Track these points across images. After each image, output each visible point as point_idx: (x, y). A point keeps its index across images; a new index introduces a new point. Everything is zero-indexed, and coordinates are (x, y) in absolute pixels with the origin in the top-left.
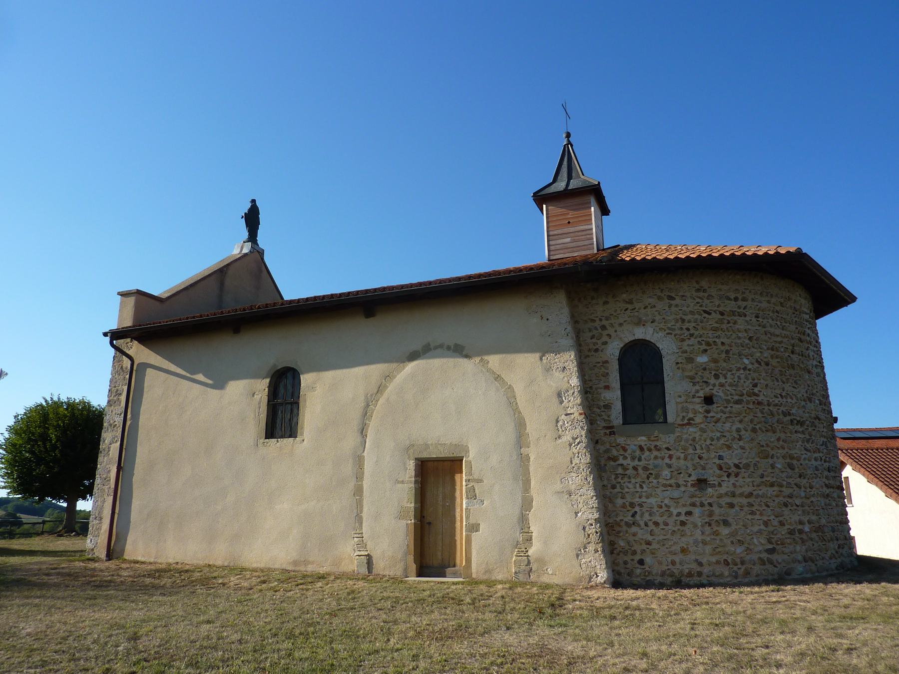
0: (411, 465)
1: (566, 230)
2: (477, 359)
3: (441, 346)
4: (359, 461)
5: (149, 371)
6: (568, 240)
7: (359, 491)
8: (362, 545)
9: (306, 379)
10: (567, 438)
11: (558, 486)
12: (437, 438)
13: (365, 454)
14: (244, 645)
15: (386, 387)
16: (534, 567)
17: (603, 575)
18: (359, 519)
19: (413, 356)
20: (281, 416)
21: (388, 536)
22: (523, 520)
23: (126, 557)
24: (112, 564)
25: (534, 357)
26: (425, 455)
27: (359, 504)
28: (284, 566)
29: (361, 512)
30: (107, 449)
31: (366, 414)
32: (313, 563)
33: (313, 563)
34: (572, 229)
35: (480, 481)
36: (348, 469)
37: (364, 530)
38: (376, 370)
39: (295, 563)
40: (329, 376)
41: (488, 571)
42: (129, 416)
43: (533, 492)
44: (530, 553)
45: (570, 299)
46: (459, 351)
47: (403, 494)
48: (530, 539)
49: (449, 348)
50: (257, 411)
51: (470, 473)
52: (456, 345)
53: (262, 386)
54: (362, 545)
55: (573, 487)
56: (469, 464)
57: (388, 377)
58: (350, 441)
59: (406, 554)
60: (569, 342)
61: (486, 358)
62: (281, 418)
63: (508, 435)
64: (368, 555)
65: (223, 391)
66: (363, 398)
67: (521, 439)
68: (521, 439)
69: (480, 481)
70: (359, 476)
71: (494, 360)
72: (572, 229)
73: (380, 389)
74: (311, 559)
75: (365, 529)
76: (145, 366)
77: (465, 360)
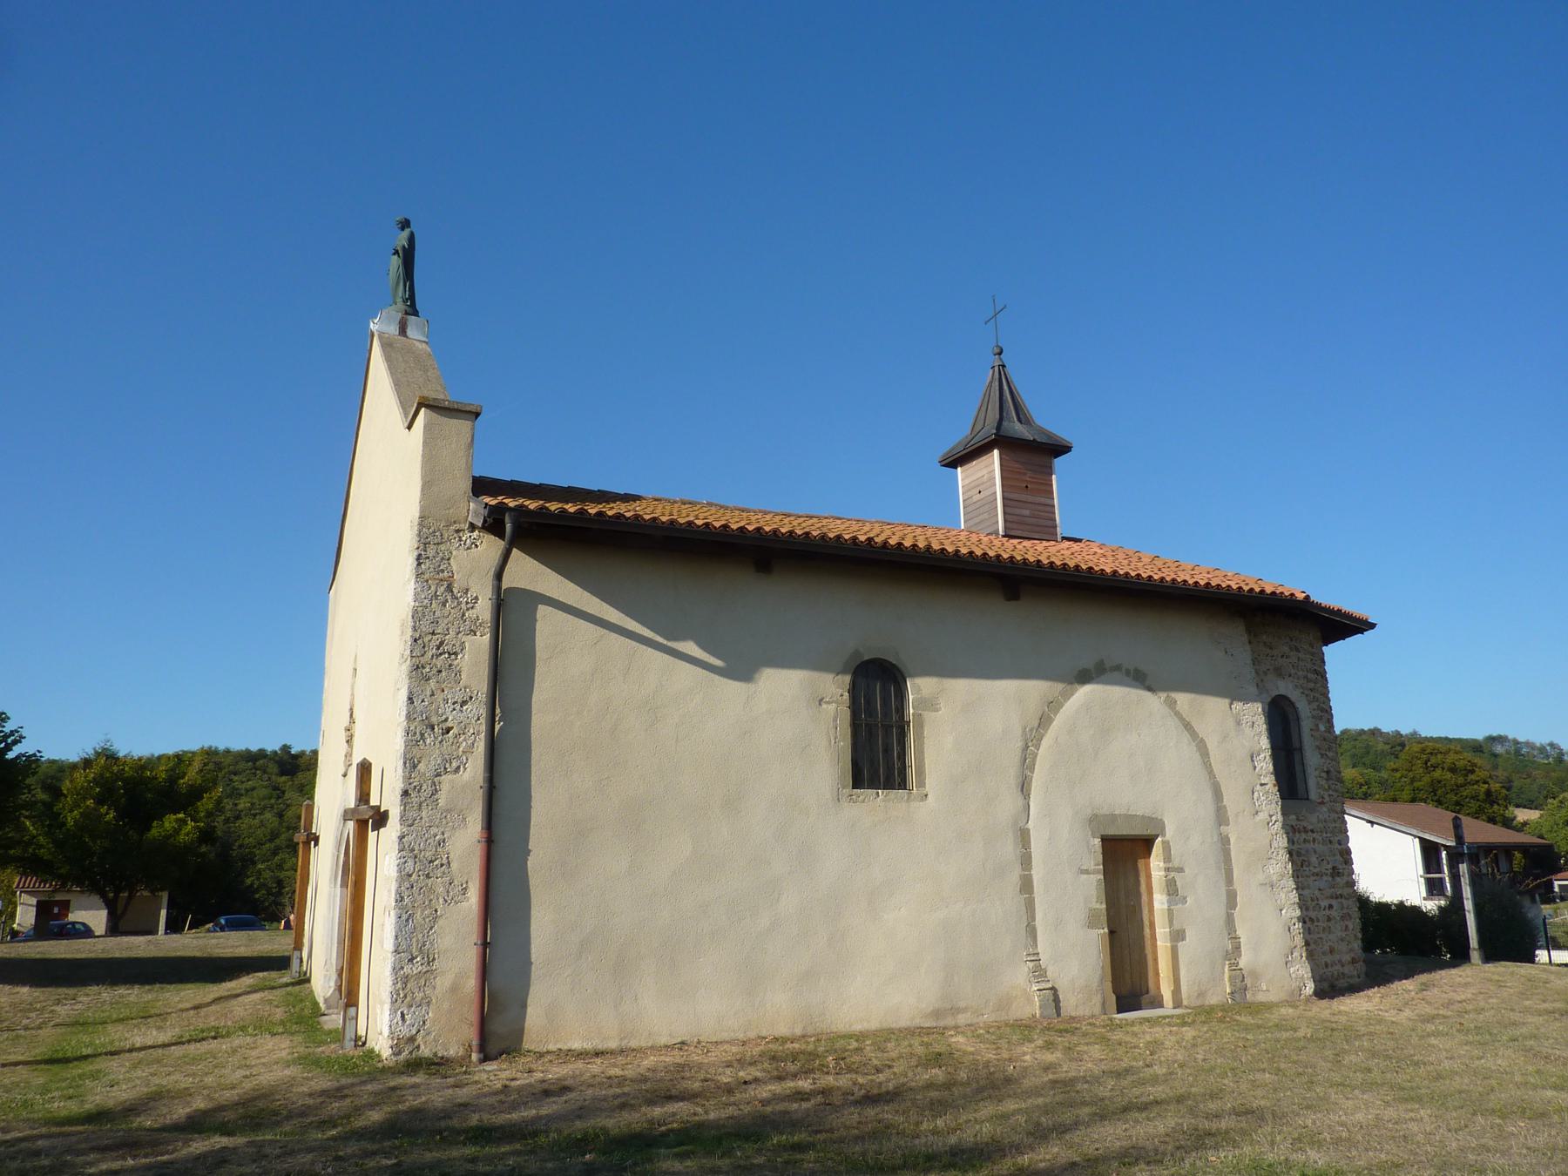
0: (1097, 842)
1: (1023, 497)
2: (1163, 695)
3: (1118, 668)
4: (1024, 837)
5: (543, 610)
6: (1027, 512)
7: (1027, 885)
8: (1039, 973)
9: (918, 688)
10: (1263, 816)
11: (1261, 877)
12: (1128, 800)
13: (1030, 825)
14: (1403, 756)
15: (1050, 721)
16: (1248, 981)
17: (1310, 987)
18: (1032, 932)
19: (1084, 677)
20: (878, 754)
21: (1075, 959)
22: (1230, 921)
23: (526, 1045)
24: (495, 1074)
25: (1223, 703)
26: (1111, 831)
27: (1030, 906)
28: (918, 1022)
29: (1034, 919)
30: (427, 789)
31: (1027, 762)
32: (965, 1010)
33: (965, 1010)
34: (1030, 498)
35: (1180, 870)
36: (1008, 849)
37: (1040, 950)
38: (1034, 690)
39: (937, 1014)
40: (961, 688)
41: (1201, 994)
42: (498, 711)
43: (1237, 885)
44: (1241, 965)
45: (1249, 631)
46: (1140, 679)
47: (1087, 889)
48: (1237, 948)
49: (1128, 673)
50: (832, 732)
51: (1167, 857)
52: (1137, 671)
53: (835, 687)
54: (1039, 973)
55: (1274, 878)
56: (1167, 847)
57: (1053, 706)
58: (1008, 803)
59: (1102, 980)
60: (1253, 690)
61: (1174, 695)
62: (878, 754)
63: (1207, 809)
64: (1053, 988)
65: (751, 686)
66: (1019, 732)
67: (1221, 817)
68: (1221, 817)
69: (1180, 870)
70: (1026, 861)
71: (1183, 699)
72: (1030, 498)
73: (1044, 722)
74: (962, 1004)
75: (1042, 946)
76: (536, 599)
77: (1148, 694)
